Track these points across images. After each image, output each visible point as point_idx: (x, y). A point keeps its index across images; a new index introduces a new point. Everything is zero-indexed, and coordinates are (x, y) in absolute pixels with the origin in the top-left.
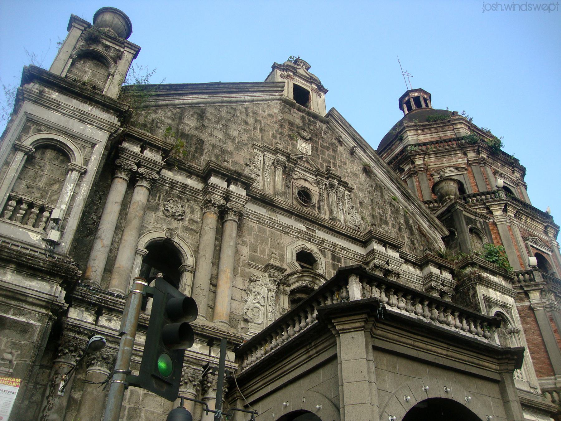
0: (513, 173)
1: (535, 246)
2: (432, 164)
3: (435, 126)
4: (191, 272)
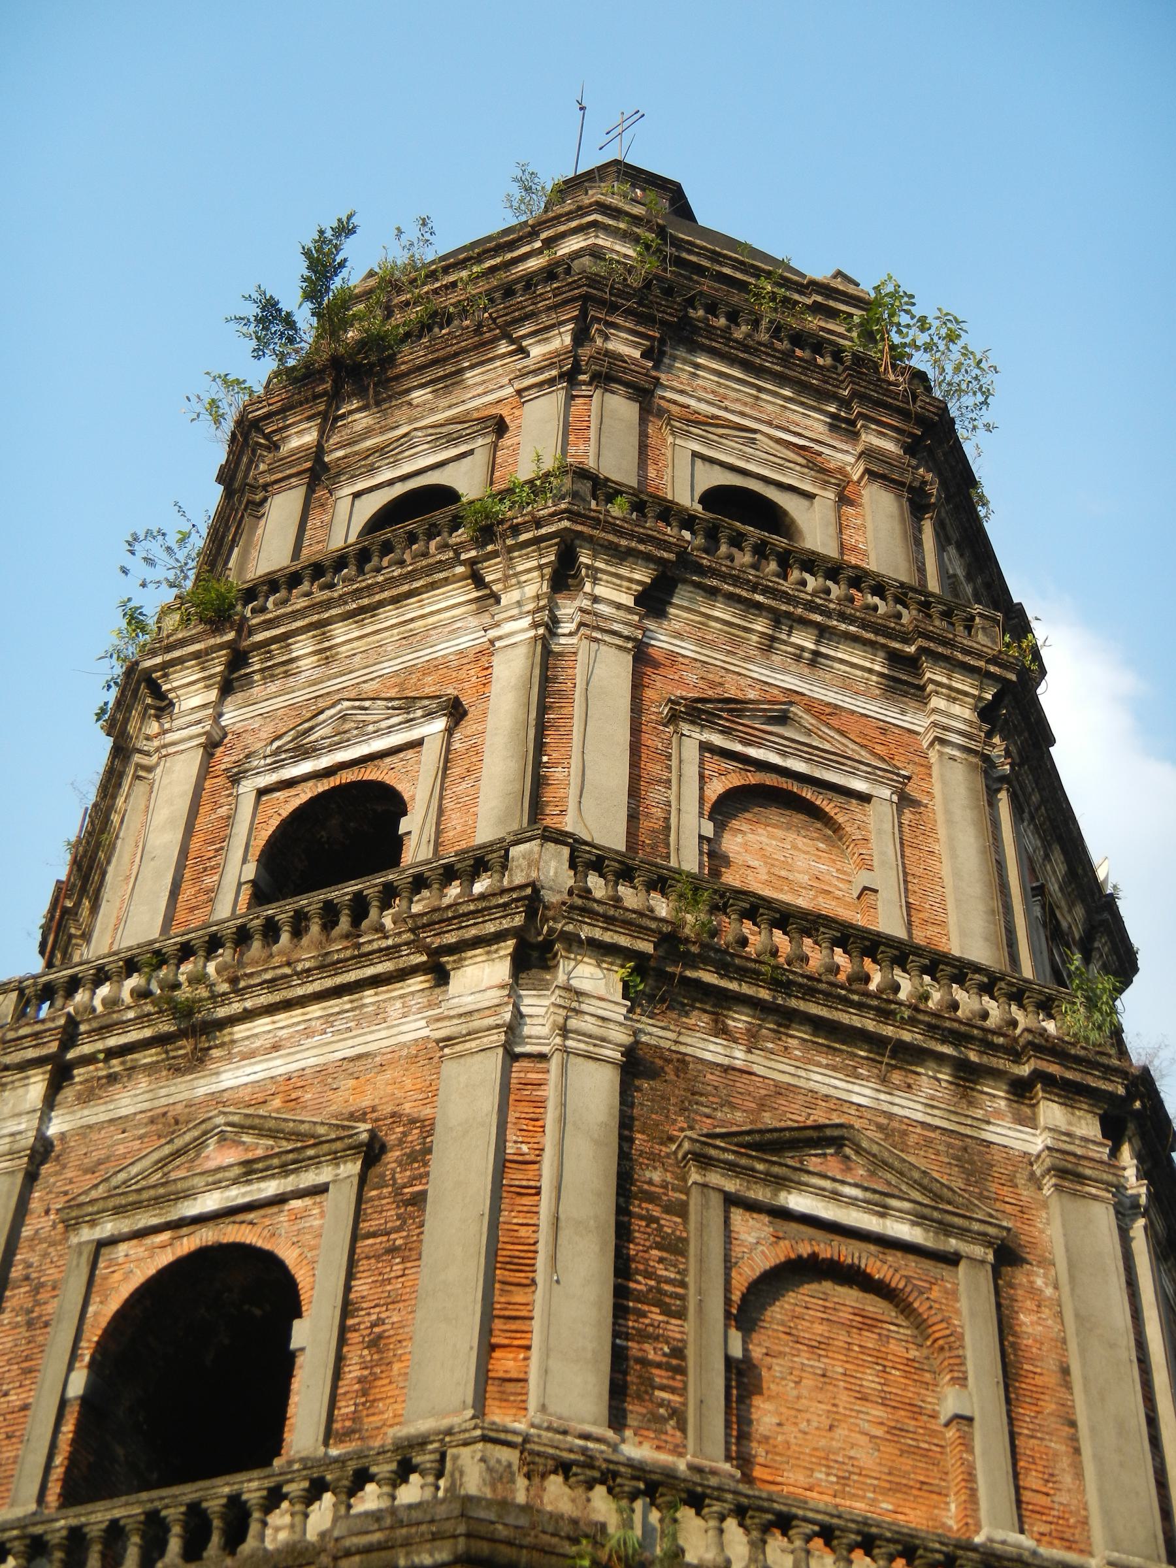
1: (306, 767)
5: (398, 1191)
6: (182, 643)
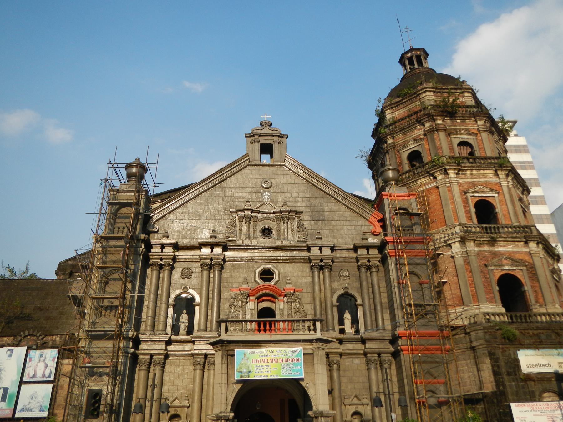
0: (477, 122)
1: (477, 195)
2: (399, 140)
3: (405, 100)
4: (198, 305)
5: (530, 272)
6: (452, 166)
